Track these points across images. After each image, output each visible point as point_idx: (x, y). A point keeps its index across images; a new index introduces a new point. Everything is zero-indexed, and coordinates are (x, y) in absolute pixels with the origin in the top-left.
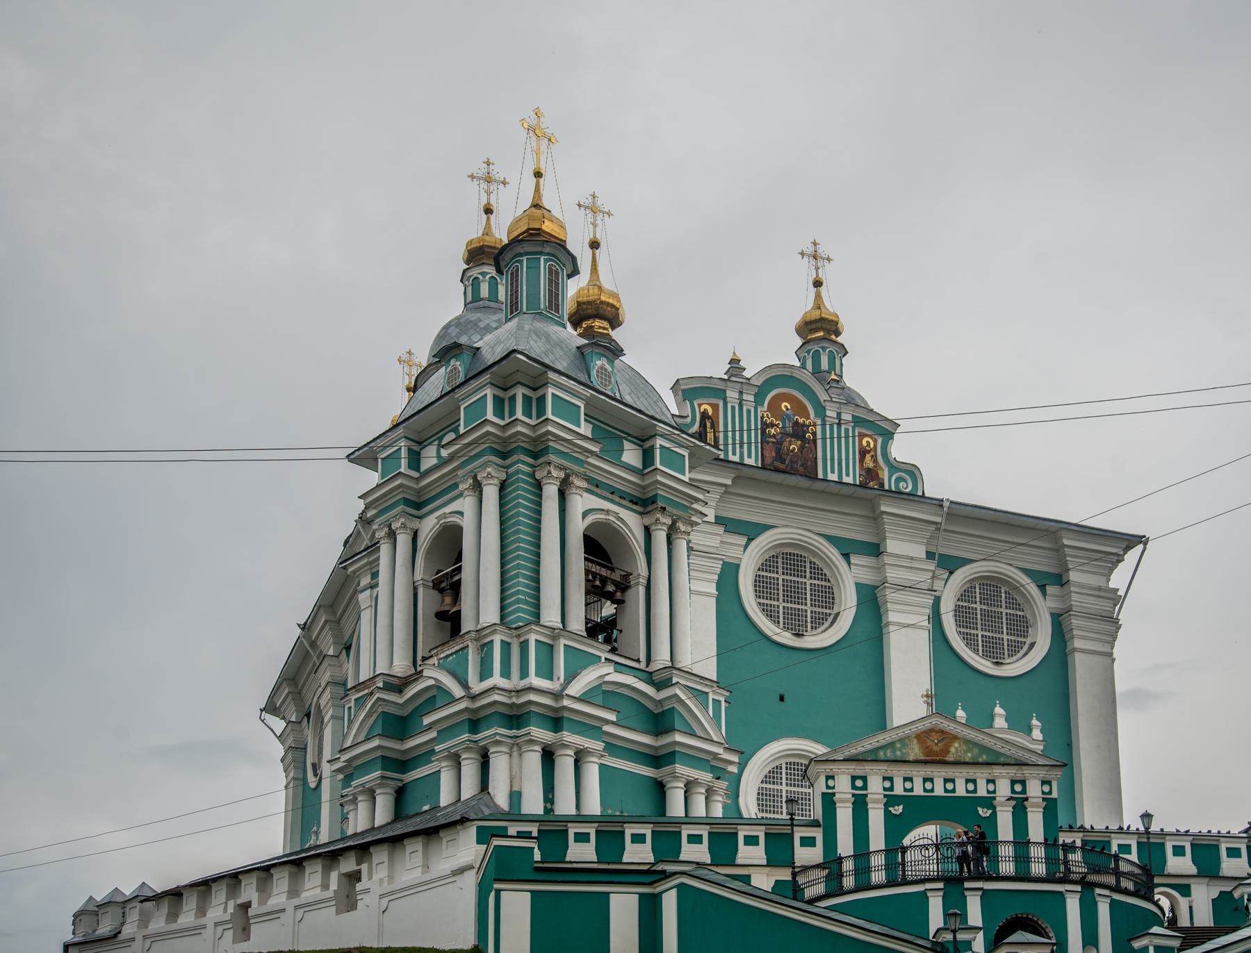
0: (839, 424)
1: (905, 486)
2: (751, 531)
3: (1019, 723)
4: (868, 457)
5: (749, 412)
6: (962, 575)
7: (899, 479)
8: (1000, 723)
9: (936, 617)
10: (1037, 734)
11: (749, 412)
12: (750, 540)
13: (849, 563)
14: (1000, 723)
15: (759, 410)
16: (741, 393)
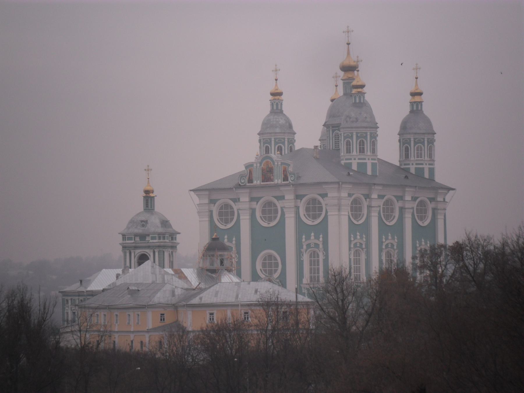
0: (278, 166)
1: (292, 178)
2: (257, 200)
3: (317, 237)
4: (285, 172)
5: (258, 168)
6: (304, 199)
7: (291, 177)
8: (312, 238)
9: (297, 213)
10: (321, 239)
11: (258, 168)
12: (257, 202)
13: (279, 203)
14: (312, 238)
15: (261, 167)
16: (257, 164)
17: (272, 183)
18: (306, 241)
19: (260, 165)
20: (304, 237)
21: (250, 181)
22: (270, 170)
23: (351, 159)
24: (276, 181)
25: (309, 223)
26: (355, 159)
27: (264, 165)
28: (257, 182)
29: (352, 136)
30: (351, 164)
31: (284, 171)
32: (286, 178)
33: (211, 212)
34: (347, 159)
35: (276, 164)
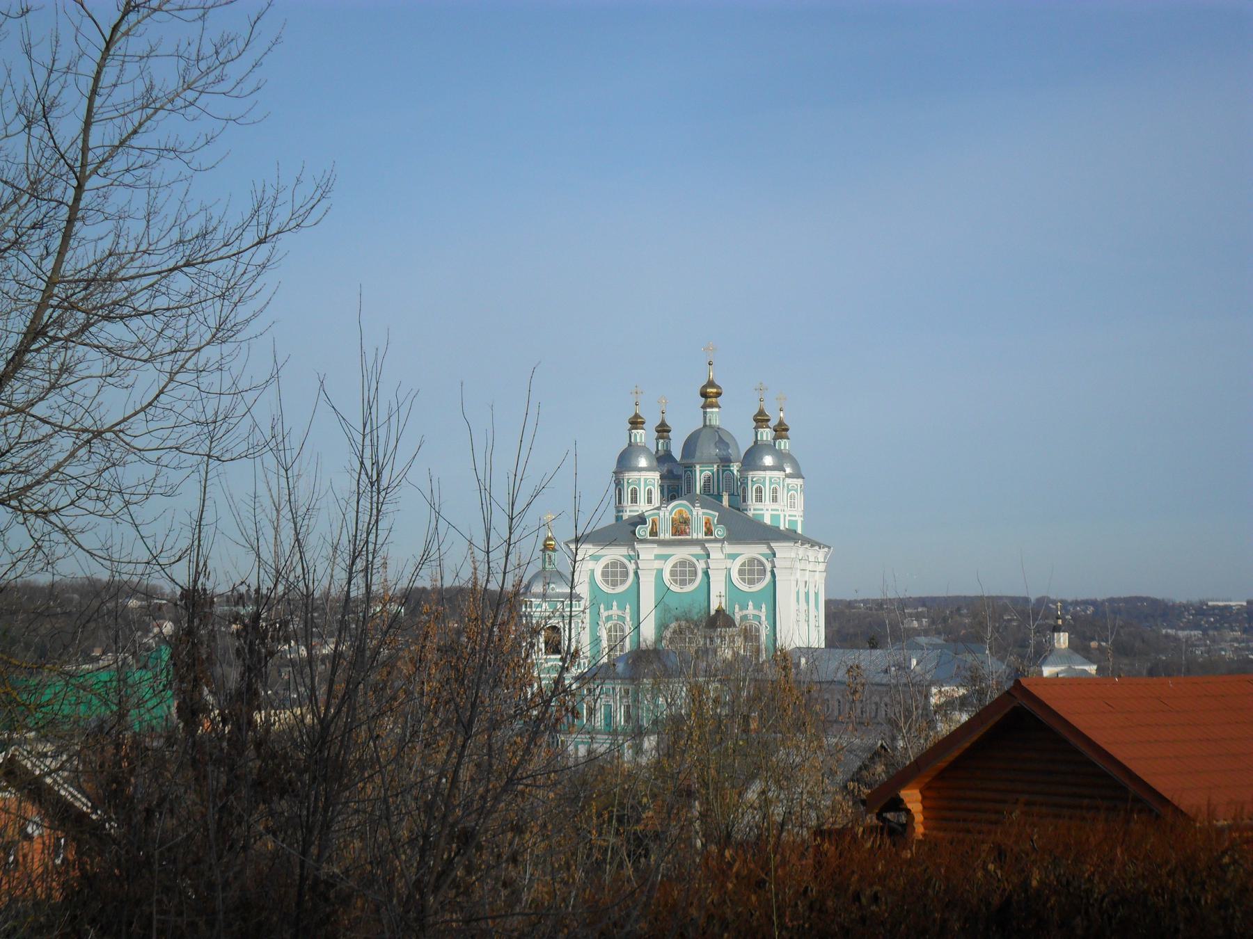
2: (665, 558)
17: (687, 537)
18: (741, 609)
19: (671, 513)
20: (737, 606)
21: (654, 533)
22: (686, 522)
23: (762, 510)
24: (695, 536)
25: (745, 587)
26: (767, 510)
27: (675, 515)
28: (666, 535)
29: (764, 481)
30: (763, 515)
31: (706, 523)
32: (709, 532)
33: (593, 571)
34: (754, 510)
35: (695, 513)
